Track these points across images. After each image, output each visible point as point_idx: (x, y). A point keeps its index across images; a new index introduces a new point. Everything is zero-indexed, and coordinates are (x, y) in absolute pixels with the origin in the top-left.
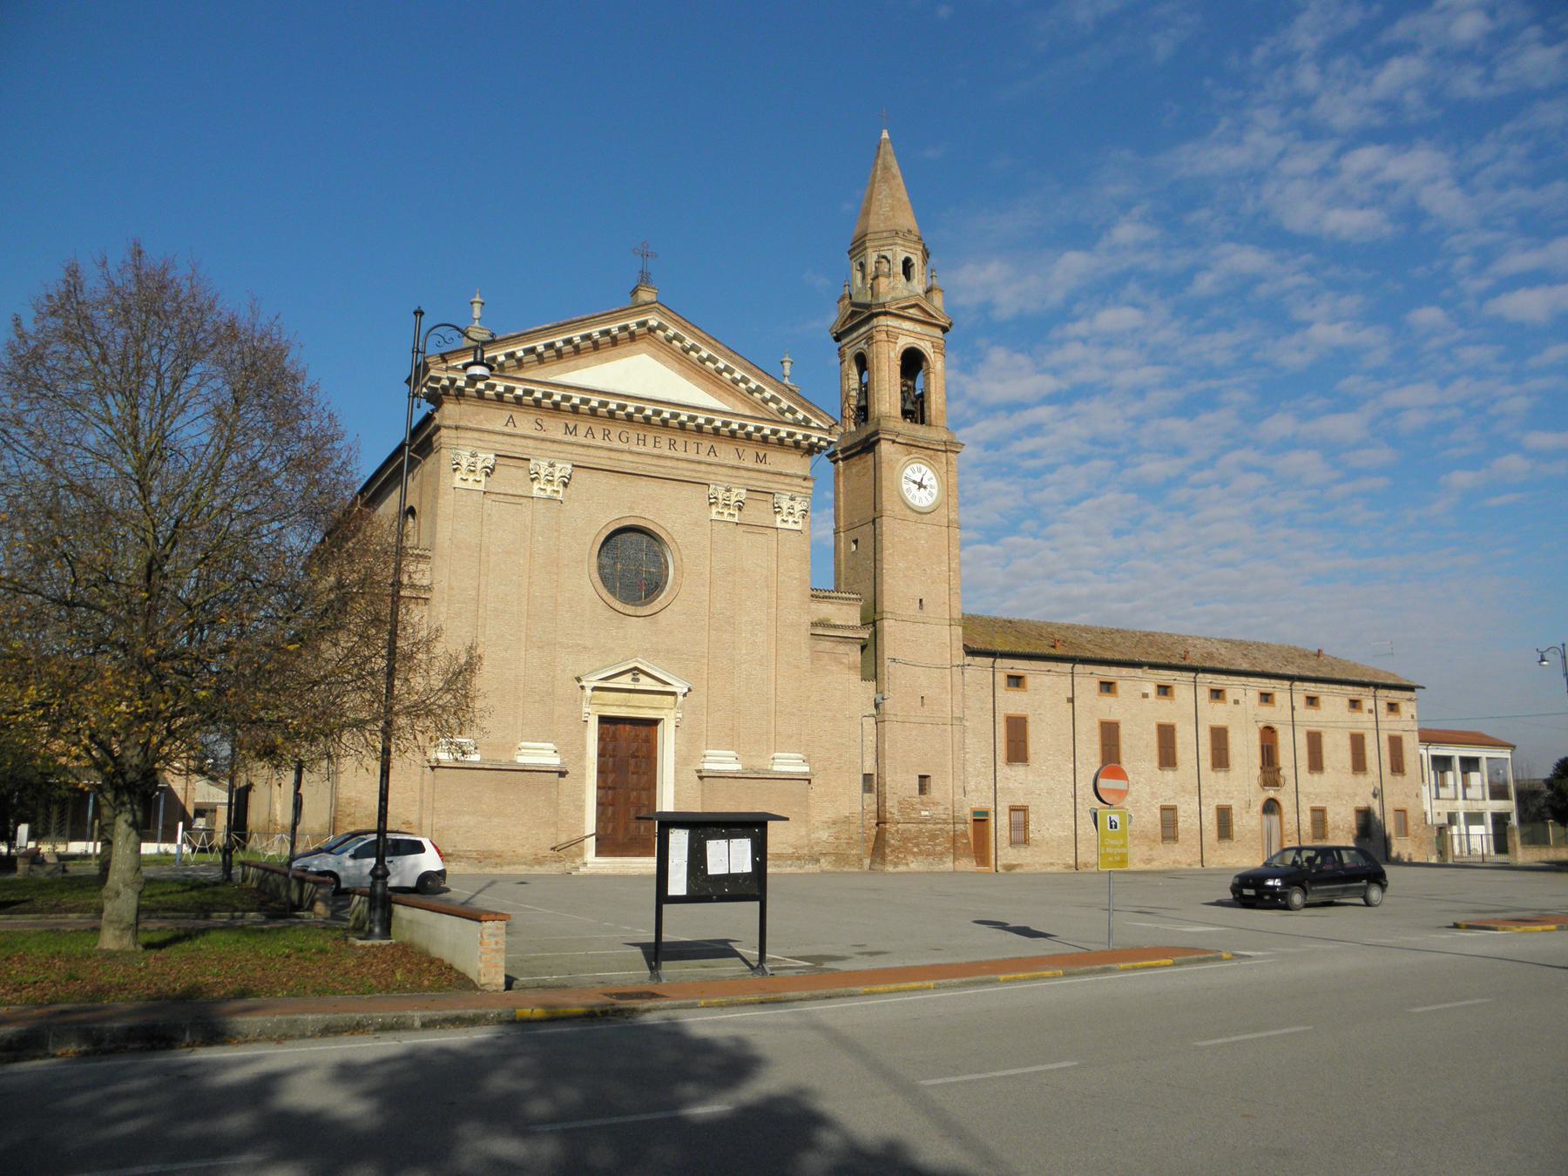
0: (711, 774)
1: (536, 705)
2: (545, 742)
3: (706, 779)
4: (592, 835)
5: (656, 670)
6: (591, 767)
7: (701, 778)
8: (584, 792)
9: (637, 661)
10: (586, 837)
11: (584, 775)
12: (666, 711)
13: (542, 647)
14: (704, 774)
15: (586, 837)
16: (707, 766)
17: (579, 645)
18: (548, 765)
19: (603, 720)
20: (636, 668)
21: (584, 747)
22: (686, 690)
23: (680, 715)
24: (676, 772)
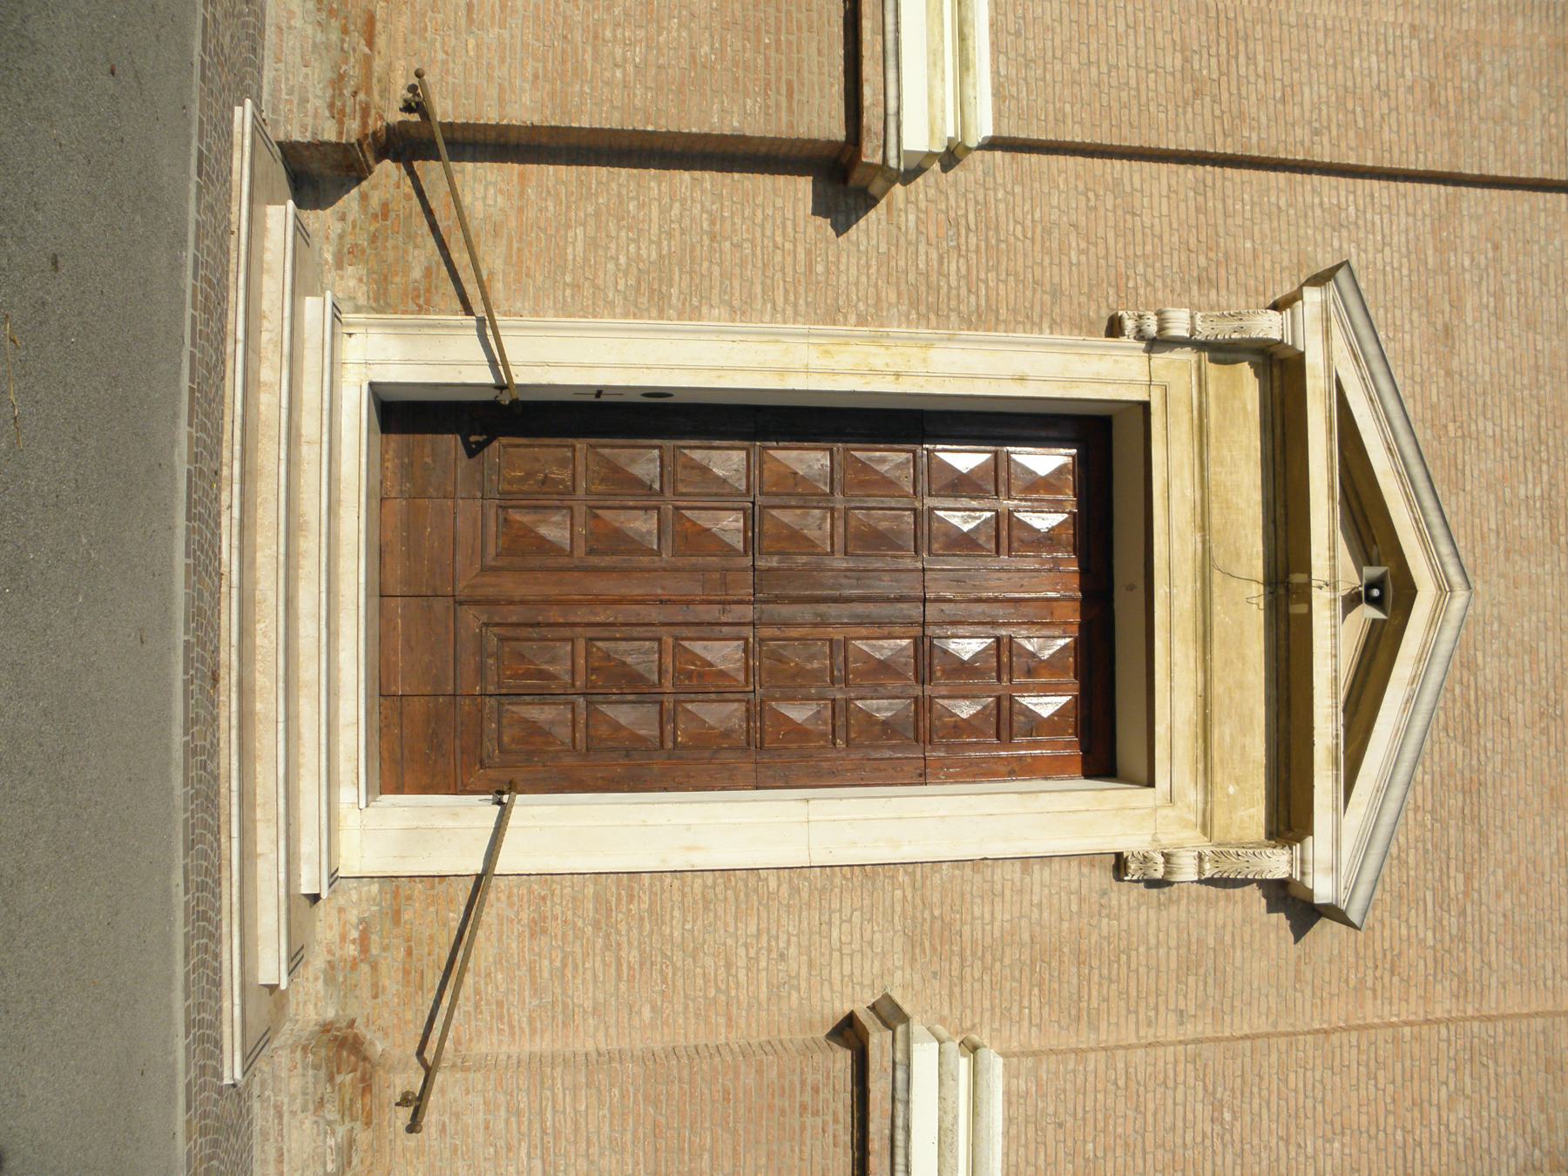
0: (878, 1088)
1: (1173, 61)
2: (998, 93)
3: (843, 1059)
4: (497, 361)
5: (1412, 700)
6: (879, 357)
7: (849, 1032)
8: (740, 310)
9: (1444, 588)
10: (486, 329)
11: (832, 315)
12: (1192, 795)
13: (1433, 103)
14: (878, 1040)
15: (486, 329)
16: (925, 1057)
17: (1457, 305)
18: (892, 56)
19: (1145, 407)
20: (1407, 592)
21: (983, 318)
22: (1323, 890)
23: (1187, 871)
24: (868, 871)
